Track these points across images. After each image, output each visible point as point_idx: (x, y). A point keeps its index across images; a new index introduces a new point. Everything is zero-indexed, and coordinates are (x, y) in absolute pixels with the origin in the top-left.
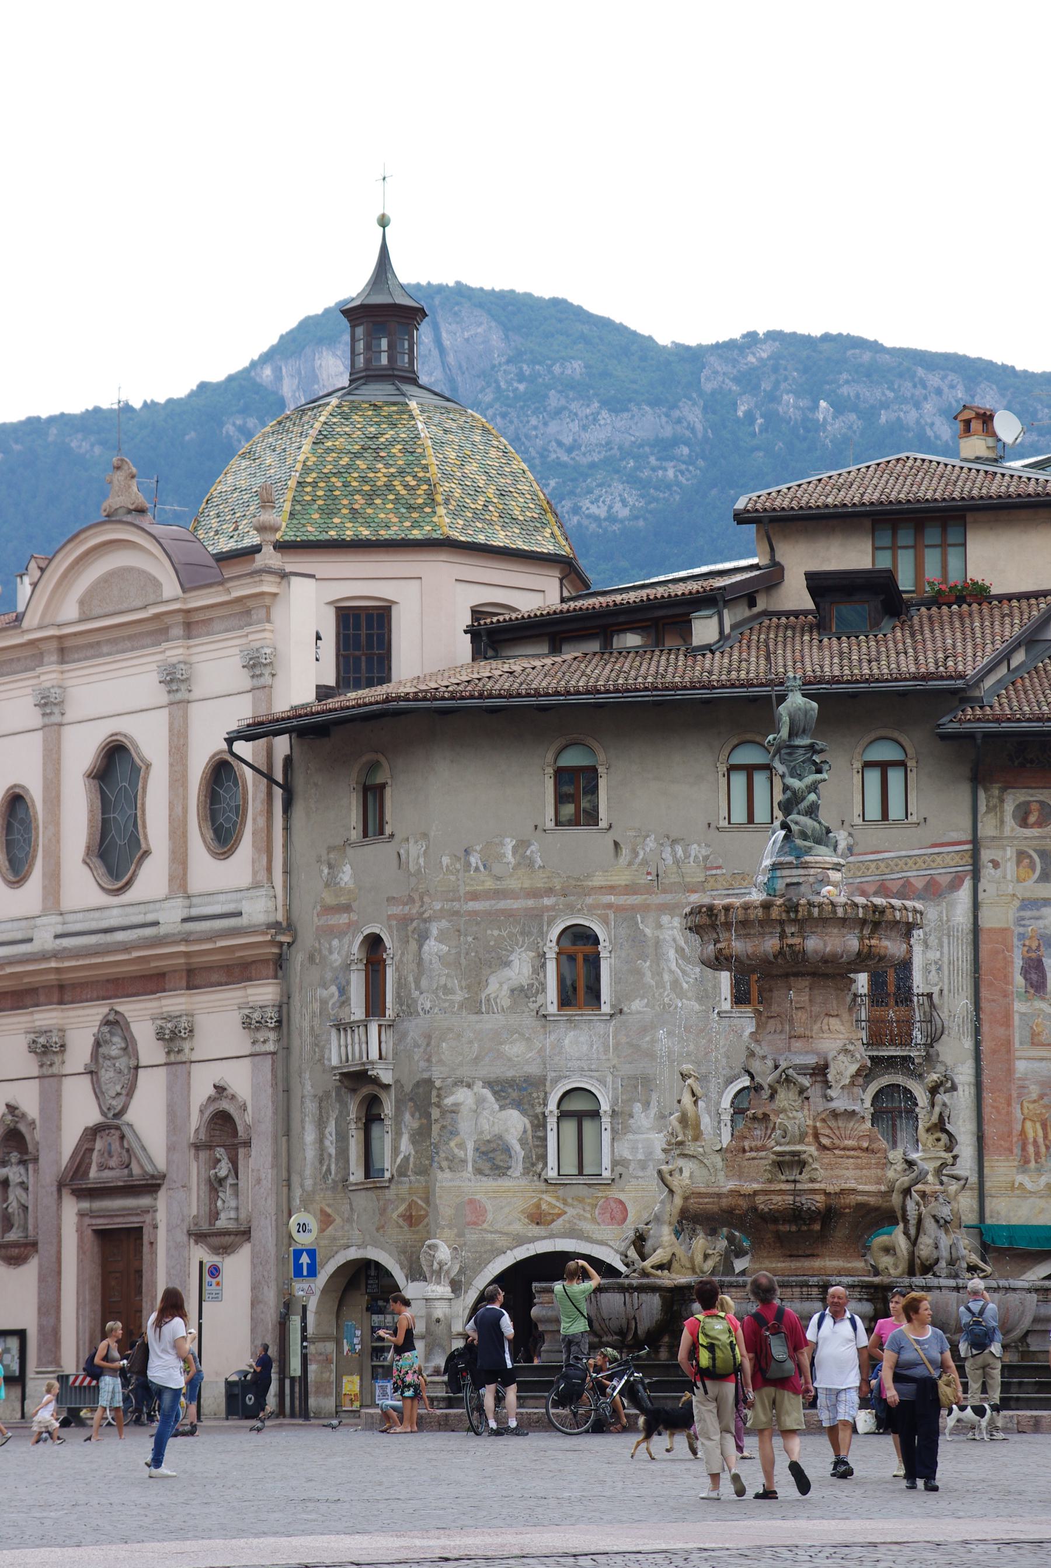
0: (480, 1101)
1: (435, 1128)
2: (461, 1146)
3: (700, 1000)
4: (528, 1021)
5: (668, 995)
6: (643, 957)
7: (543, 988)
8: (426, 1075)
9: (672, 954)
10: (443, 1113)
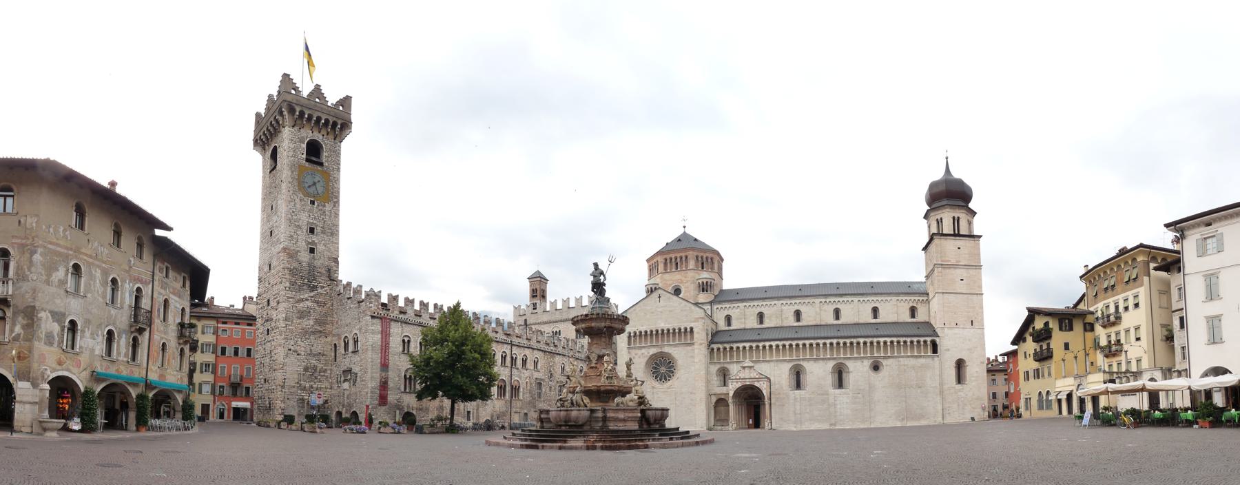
0: (47, 318)
1: (35, 324)
2: (41, 333)
3: (103, 298)
4: (62, 292)
5: (96, 295)
6: (91, 280)
7: (67, 283)
8: (32, 304)
9: (98, 282)
10: (38, 319)
